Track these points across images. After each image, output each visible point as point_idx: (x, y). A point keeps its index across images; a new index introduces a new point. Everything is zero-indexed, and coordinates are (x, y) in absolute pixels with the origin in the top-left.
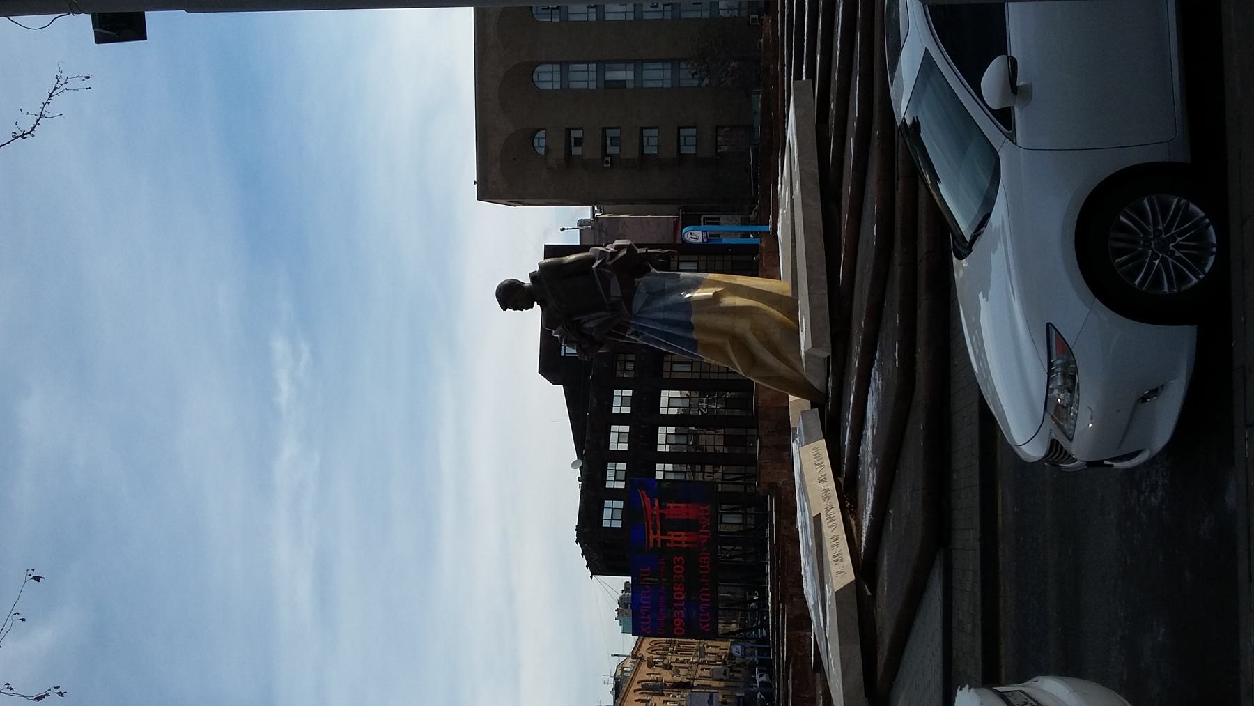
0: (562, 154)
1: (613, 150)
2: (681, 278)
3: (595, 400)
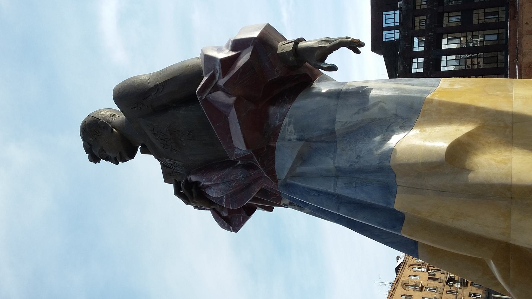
2: (371, 102)
3: (401, 67)
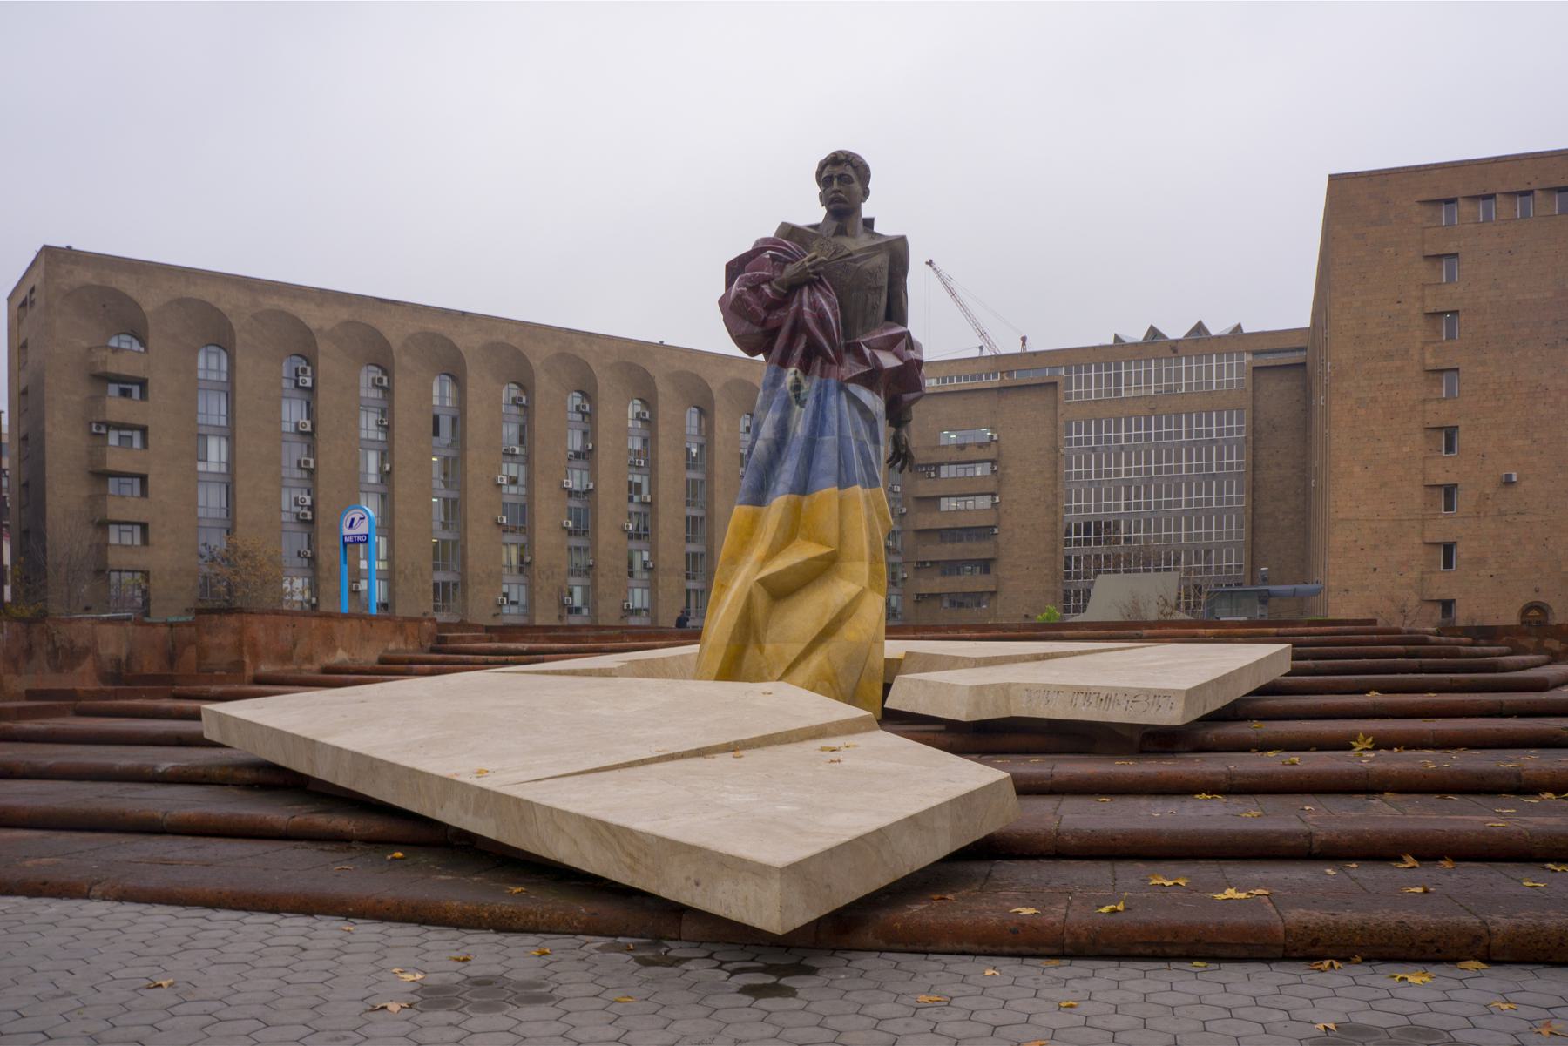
0: (112, 368)
1: (113, 438)
